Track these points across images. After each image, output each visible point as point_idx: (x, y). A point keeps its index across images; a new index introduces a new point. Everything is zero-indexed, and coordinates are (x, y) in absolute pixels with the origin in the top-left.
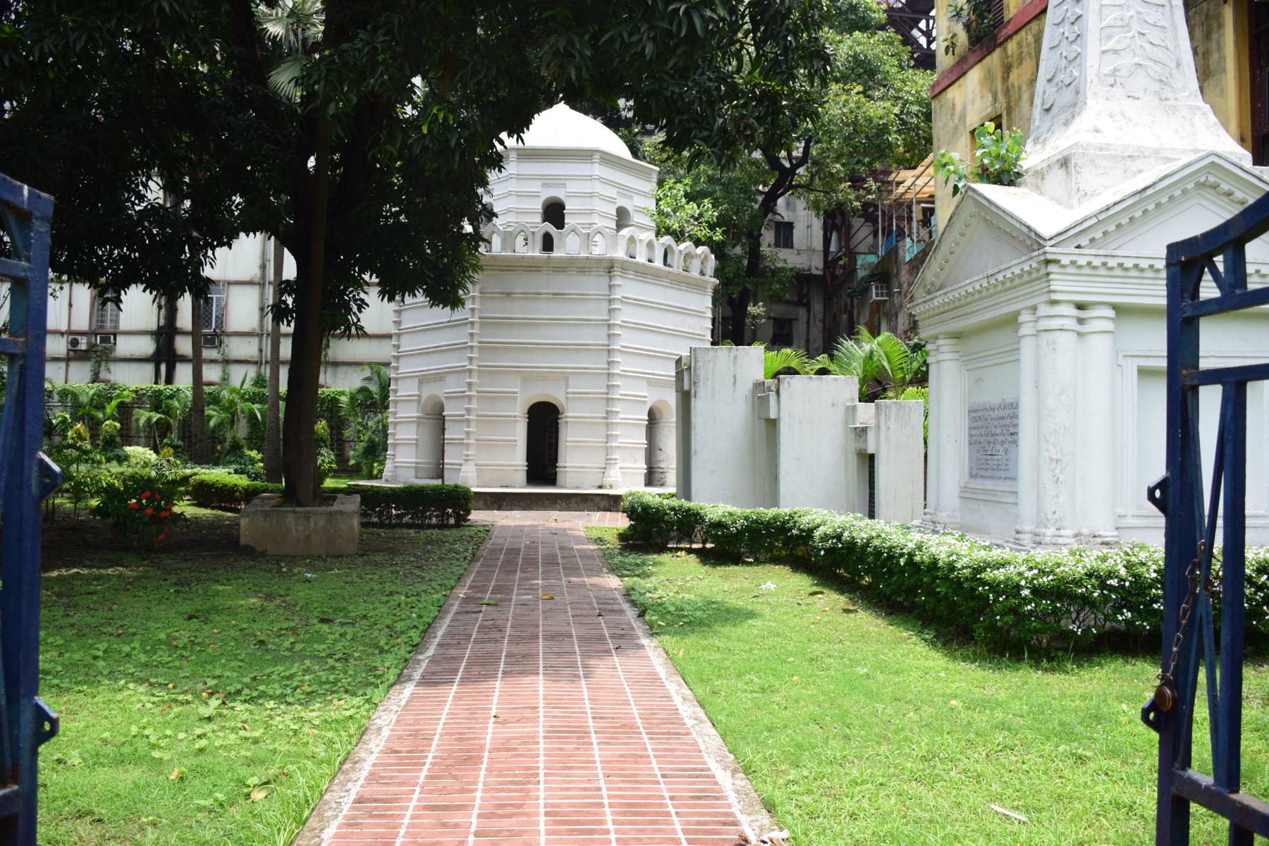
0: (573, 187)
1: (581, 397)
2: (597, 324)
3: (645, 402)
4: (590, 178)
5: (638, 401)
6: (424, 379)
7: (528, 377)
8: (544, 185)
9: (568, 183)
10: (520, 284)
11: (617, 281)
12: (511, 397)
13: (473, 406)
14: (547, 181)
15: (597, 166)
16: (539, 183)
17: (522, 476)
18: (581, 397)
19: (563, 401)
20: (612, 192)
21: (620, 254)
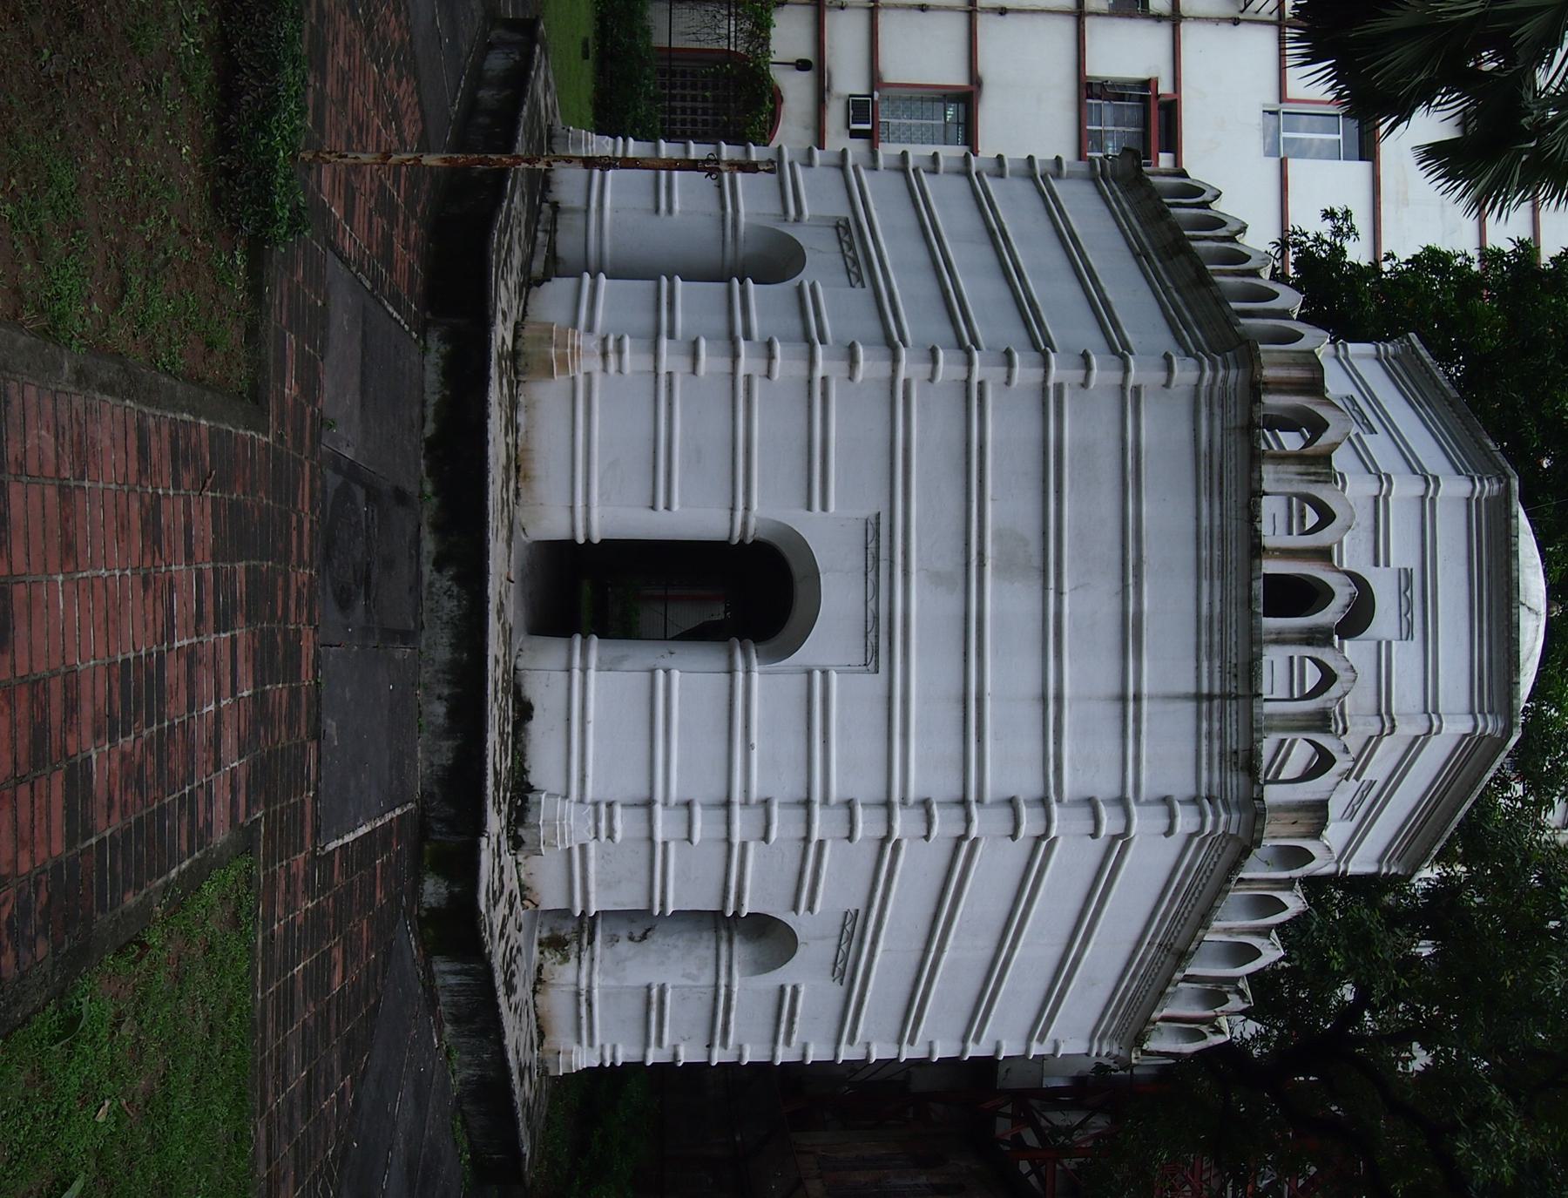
0: (1406, 658)
1: (811, 713)
2: (1050, 763)
3: (795, 908)
4: (1431, 708)
5: (802, 889)
6: (850, 235)
7: (879, 546)
8: (1408, 574)
9: (1415, 645)
10: (1170, 514)
11: (1186, 821)
12: (812, 490)
13: (786, 363)
14: (1418, 588)
15: (1465, 726)
16: (1413, 563)
17: (551, 523)
18: (811, 713)
19: (806, 654)
20: (1377, 770)
21: (1276, 835)
